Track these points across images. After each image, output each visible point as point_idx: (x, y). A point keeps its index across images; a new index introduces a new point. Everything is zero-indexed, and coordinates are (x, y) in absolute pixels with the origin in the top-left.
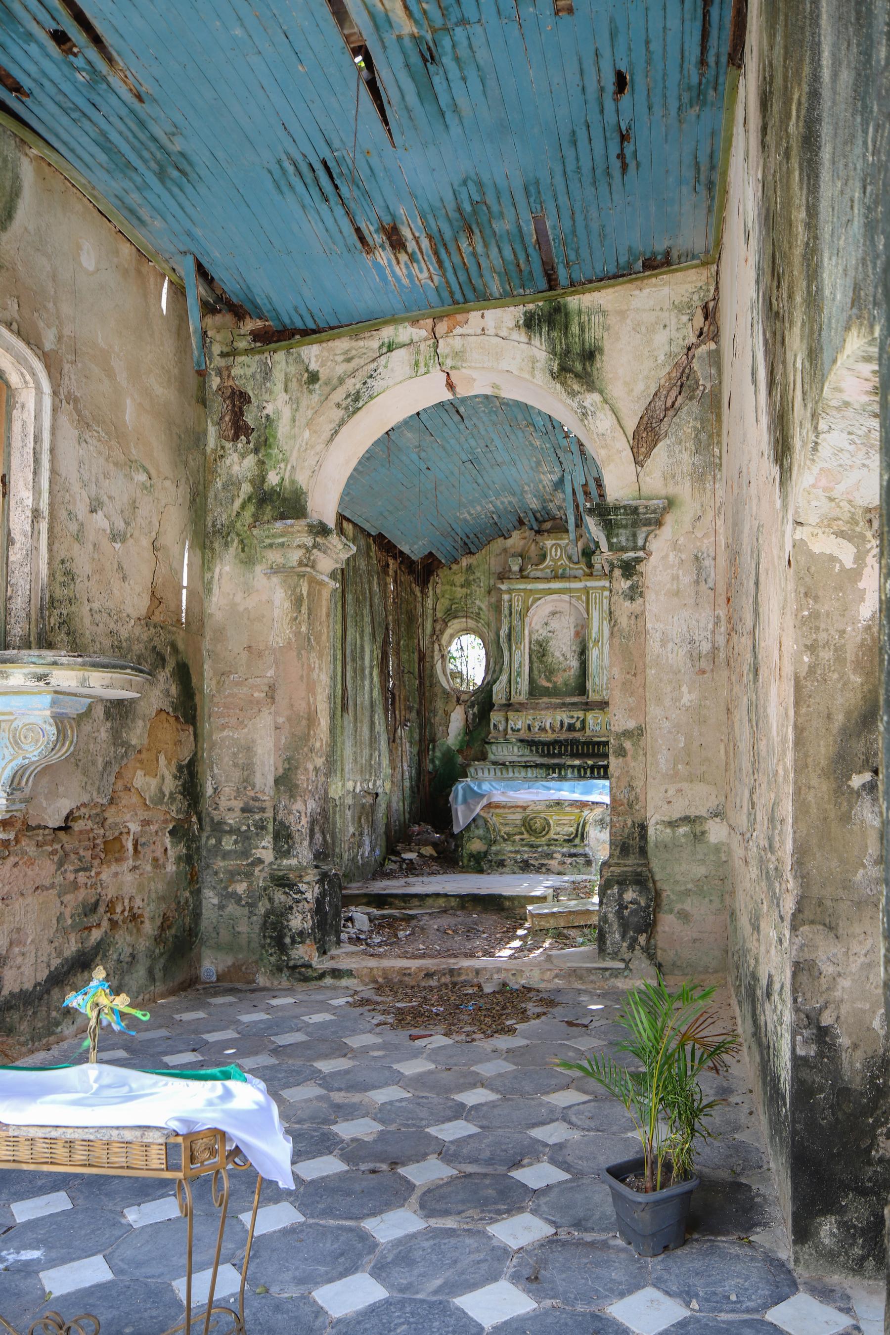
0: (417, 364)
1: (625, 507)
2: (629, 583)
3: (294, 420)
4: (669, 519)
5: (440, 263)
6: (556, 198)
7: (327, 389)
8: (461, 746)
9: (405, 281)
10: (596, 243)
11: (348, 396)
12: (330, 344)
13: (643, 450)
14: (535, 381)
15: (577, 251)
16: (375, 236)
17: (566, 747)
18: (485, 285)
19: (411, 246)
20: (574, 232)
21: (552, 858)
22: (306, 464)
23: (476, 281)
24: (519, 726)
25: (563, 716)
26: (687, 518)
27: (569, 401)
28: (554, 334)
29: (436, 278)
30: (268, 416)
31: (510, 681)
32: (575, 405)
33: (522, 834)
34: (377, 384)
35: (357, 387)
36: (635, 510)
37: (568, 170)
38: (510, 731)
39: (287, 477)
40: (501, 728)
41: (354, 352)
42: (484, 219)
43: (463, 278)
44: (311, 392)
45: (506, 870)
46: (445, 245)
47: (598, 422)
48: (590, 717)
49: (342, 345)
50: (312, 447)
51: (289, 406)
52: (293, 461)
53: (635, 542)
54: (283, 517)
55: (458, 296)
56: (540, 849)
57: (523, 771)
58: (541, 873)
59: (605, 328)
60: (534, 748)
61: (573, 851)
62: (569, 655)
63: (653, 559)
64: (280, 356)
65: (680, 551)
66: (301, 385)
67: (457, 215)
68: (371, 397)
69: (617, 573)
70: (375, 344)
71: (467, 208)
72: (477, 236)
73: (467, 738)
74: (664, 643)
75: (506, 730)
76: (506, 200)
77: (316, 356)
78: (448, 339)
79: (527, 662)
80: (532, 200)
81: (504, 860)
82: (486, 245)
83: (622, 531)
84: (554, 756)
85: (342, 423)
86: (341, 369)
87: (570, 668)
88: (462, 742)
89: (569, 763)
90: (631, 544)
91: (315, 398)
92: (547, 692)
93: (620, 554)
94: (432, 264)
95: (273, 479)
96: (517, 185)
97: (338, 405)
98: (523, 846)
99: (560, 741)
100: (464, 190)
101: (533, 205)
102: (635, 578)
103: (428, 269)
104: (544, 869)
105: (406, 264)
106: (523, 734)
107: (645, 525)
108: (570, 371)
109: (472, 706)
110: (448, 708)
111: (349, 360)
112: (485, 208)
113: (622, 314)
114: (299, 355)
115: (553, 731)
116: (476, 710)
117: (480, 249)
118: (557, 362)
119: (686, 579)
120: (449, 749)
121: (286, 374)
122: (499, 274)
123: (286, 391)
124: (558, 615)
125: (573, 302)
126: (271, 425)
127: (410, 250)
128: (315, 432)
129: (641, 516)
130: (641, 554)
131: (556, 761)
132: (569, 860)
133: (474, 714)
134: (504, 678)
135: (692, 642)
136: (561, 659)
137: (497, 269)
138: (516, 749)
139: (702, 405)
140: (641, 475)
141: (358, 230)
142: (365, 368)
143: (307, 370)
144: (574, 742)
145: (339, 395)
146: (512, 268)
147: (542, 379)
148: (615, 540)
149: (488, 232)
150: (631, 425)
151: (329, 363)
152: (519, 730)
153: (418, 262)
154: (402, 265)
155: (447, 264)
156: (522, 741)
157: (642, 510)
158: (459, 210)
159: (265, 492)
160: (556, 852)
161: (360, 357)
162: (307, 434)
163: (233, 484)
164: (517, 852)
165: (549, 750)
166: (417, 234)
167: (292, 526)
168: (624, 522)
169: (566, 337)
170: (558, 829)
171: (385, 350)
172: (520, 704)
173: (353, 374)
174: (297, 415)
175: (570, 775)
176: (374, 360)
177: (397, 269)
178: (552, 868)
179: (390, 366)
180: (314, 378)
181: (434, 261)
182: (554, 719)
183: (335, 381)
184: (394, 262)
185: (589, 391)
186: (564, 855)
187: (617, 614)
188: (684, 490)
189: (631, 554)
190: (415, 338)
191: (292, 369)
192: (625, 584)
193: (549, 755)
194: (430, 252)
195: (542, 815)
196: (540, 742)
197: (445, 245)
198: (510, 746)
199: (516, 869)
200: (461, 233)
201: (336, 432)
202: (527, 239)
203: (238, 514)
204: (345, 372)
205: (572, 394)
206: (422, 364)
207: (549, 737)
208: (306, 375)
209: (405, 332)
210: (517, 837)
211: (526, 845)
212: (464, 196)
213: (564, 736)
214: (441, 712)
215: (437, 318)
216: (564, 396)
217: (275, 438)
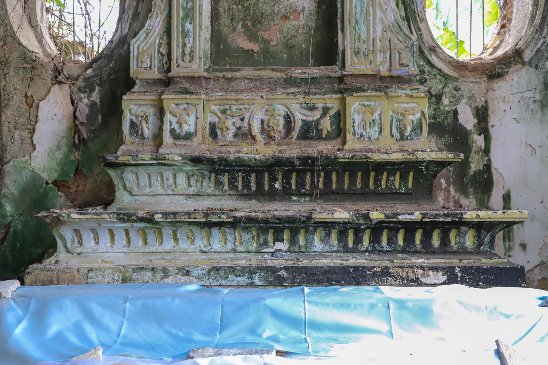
8: (63, 173)
17: (301, 174)
31: (168, 32)
38: (167, 138)
40: (147, 133)
60: (225, 179)
73: (77, 155)
88: (65, 162)
99: (289, 162)
109: (88, 88)
110: (35, 91)
115: (269, 138)
116: (96, 96)
120: (35, 178)
133: (92, 105)
138: (182, 180)
152: (189, 136)
156: (196, 160)
165: (259, 184)
172: (192, 79)
182: (270, 112)
198: (168, 173)
214: (17, 100)
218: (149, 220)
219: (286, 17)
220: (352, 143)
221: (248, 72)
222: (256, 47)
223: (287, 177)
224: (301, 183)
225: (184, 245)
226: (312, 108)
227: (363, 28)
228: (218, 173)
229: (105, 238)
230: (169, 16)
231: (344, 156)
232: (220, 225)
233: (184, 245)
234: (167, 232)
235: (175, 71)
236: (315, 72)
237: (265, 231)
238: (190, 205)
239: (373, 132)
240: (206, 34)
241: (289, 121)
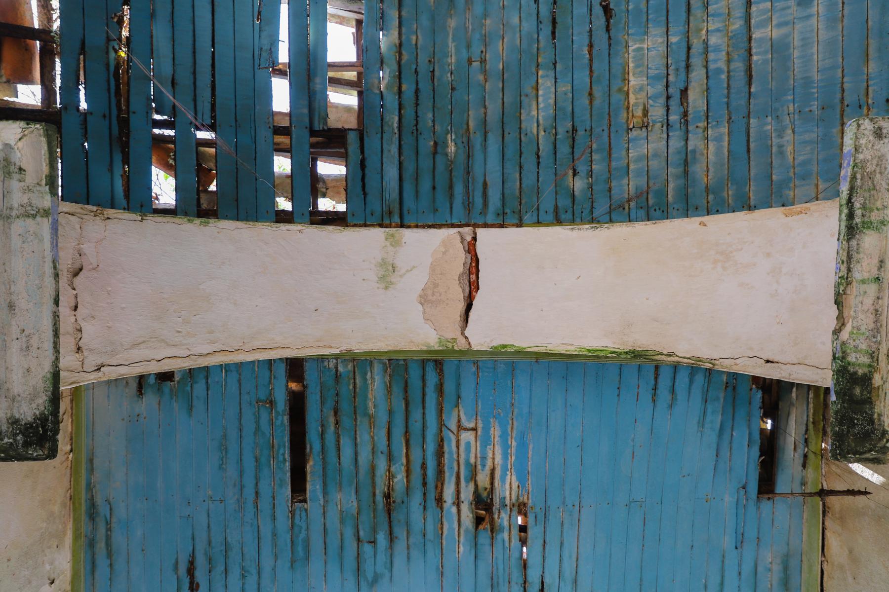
5: (440, 453)
6: (274, 534)
9: (496, 432)
10: (233, 434)
15: (258, 428)
18: (389, 391)
19: (467, 493)
20: (258, 468)
23: (399, 406)
29: (453, 426)
37: (255, 577)
42: (366, 519)
43: (416, 415)
55: (432, 379)
71: (382, 538)
72: (381, 488)
76: (334, 541)
80: (303, 535)
82: (373, 469)
94: (451, 453)
96: (316, 564)
100: (380, 568)
101: (303, 525)
105: (484, 466)
112: (361, 533)
117: (382, 465)
122: (366, 414)
137: (366, 421)
146: (346, 421)
149: (366, 494)
153: (467, 463)
154: (489, 463)
155: (431, 448)
181: (446, 456)
194: (447, 474)
197: (424, 484)
200: (398, 500)
202: (319, 468)
212: (382, 557)
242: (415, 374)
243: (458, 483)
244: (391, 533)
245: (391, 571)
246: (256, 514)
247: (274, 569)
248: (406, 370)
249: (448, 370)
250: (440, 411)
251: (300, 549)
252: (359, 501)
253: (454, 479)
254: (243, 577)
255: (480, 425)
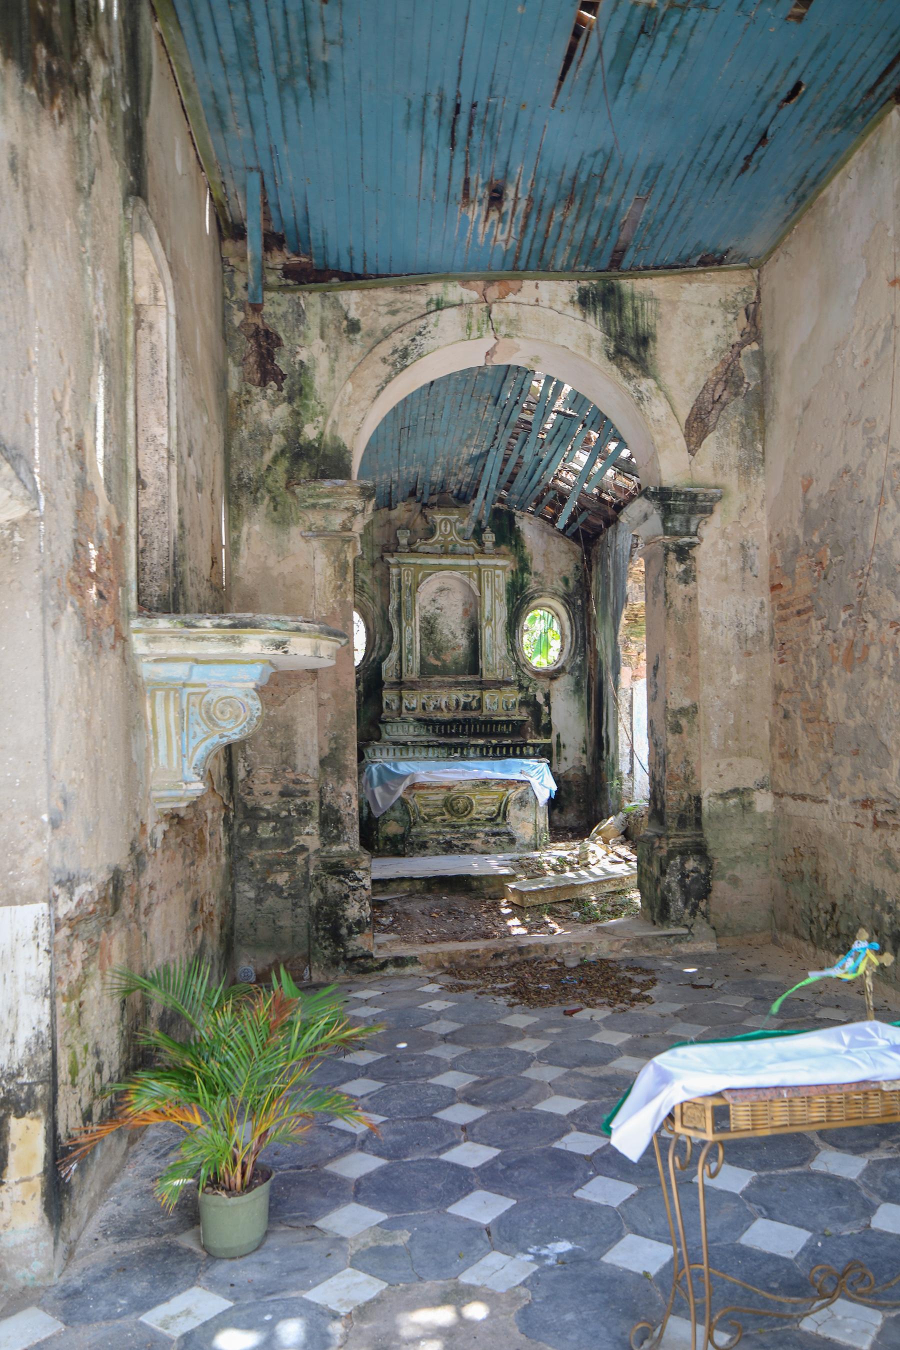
0: (469, 327)
1: (686, 494)
2: (683, 567)
3: (332, 371)
4: (718, 508)
5: (525, 227)
6: (668, 185)
7: (370, 341)
9: (481, 240)
11: (395, 351)
12: (372, 292)
13: (693, 439)
14: (591, 359)
16: (480, 190)
17: (464, 726)
19: (507, 206)
21: (475, 838)
22: (350, 420)
23: (548, 251)
24: (414, 705)
25: (460, 695)
26: (734, 508)
27: (625, 384)
28: (609, 315)
29: (511, 241)
30: (301, 363)
31: (400, 659)
32: (631, 388)
33: (443, 814)
34: (426, 343)
35: (406, 342)
36: (694, 497)
39: (327, 431)
41: (399, 305)
43: (537, 245)
44: (351, 342)
45: (429, 851)
46: (540, 211)
47: (653, 408)
48: (487, 696)
49: (385, 295)
50: (357, 402)
51: (326, 354)
52: (334, 415)
53: (688, 528)
54: (324, 476)
55: (522, 264)
56: (462, 830)
57: (424, 751)
58: (465, 853)
59: (659, 316)
60: (431, 728)
61: (496, 829)
62: (459, 633)
63: (705, 546)
64: (314, 298)
65: (728, 539)
66: (340, 334)
67: (570, 184)
68: (420, 356)
69: (672, 556)
70: (423, 300)
71: (583, 178)
72: (574, 208)
74: (714, 626)
75: (399, 709)
77: (356, 303)
78: (503, 306)
79: (418, 639)
81: (426, 842)
82: (577, 218)
83: (678, 516)
84: (451, 735)
85: (388, 380)
86: (385, 321)
87: (459, 646)
89: (473, 742)
90: (684, 530)
91: (357, 349)
92: (436, 671)
93: (676, 538)
94: (516, 227)
95: (310, 432)
97: (384, 360)
98: (444, 826)
99: (459, 721)
102: (688, 562)
103: (510, 231)
104: (467, 850)
106: (419, 713)
107: (701, 512)
108: (626, 354)
111: (394, 313)
113: (673, 304)
114: (337, 300)
117: (570, 221)
118: (613, 344)
119: (734, 566)
121: (322, 319)
123: (322, 337)
124: (445, 592)
125: (627, 285)
126: (306, 373)
127: (504, 209)
128: (359, 386)
129: (699, 504)
130: (695, 539)
131: (455, 740)
132: (493, 840)
134: (394, 655)
135: (739, 625)
136: (450, 636)
139: (746, 402)
140: (693, 463)
141: (467, 182)
142: (413, 323)
143: (346, 318)
144: (467, 721)
145: (384, 349)
146: (588, 243)
147: (598, 358)
148: (670, 525)
150: (684, 413)
151: (371, 313)
154: (488, 224)
155: (531, 231)
156: (419, 720)
157: (700, 498)
158: (575, 179)
159: (301, 447)
160: (478, 832)
161: (405, 311)
162: (349, 387)
163: (261, 434)
164: (439, 833)
165: (446, 729)
166: (520, 195)
167: (342, 486)
168: (682, 508)
169: (620, 319)
170: (480, 808)
171: (433, 307)
172: (412, 682)
173: (400, 328)
174: (336, 365)
175: (472, 755)
176: (422, 316)
177: (481, 227)
178: (475, 847)
179: (440, 324)
180: (354, 327)
183: (378, 334)
184: (483, 218)
185: (644, 376)
186: (487, 834)
187: (672, 596)
188: (731, 481)
189: (687, 539)
190: (466, 300)
191: (329, 314)
192: (680, 568)
193: (446, 735)
194: (522, 215)
195: (466, 795)
196: (438, 721)
197: (540, 211)
199: (439, 850)
201: (383, 388)
203: (269, 468)
204: (389, 325)
205: (628, 377)
206: (475, 328)
207: (446, 716)
208: (345, 323)
209: (455, 292)
210: (438, 818)
211: (447, 826)
213: (460, 715)
215: (490, 281)
216: (620, 378)
217: (311, 388)
218: (405, 744)
219: (454, 649)
220: (485, 712)
221: (438, 678)
222: (439, 663)
223: (458, 727)
224: (464, 730)
225: (417, 755)
226: (468, 696)
227: (490, 658)
228: (428, 725)
229: (385, 752)
230: (401, 651)
231: (482, 718)
232: (433, 746)
233: (417, 755)
234: (411, 750)
235: (404, 678)
236: (469, 678)
237: (450, 749)
238: (415, 739)
239: (495, 707)
240: (418, 660)
241: (458, 702)
242: (533, 263)
243: (514, 210)
244: (574, 183)
245: (581, 159)
246: (677, 195)
247: (678, 165)
248: (538, 266)
249: (510, 265)
250: (520, 248)
251: (652, 173)
252: (594, 202)
253: (517, 213)
254: (706, 161)
255: (492, 243)
